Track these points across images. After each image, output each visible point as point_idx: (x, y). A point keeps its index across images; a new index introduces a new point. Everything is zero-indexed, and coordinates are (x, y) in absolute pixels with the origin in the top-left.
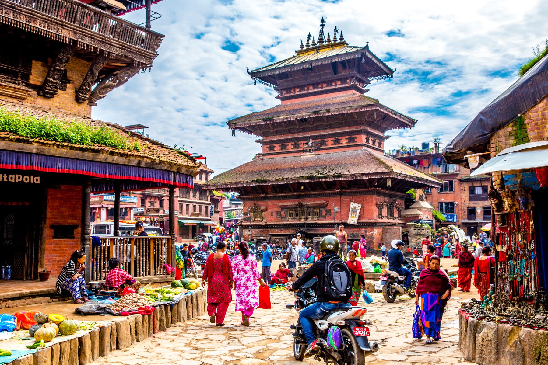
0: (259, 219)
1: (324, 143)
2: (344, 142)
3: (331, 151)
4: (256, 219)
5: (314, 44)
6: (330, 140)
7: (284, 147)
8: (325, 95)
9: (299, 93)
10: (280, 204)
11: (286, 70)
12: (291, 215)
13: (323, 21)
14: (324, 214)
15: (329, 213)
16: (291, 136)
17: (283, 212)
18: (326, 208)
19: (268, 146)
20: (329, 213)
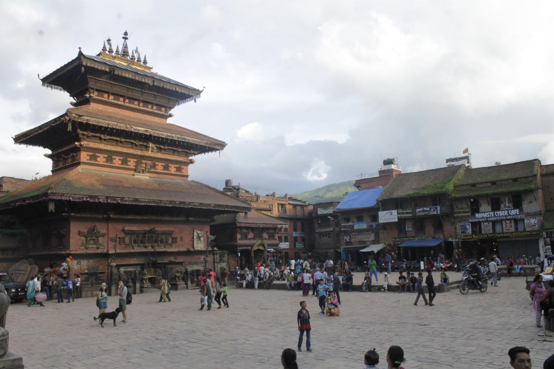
0: (95, 246)
1: (154, 166)
2: (173, 170)
3: (161, 176)
4: (90, 246)
5: (117, 51)
6: (160, 164)
7: (109, 159)
8: (140, 114)
9: (113, 101)
10: (126, 228)
11: (127, 76)
12: (135, 242)
13: (126, 34)
14: (170, 241)
15: (175, 240)
16: (118, 149)
17: (127, 239)
18: (173, 236)
19: (91, 154)
20: (175, 240)
